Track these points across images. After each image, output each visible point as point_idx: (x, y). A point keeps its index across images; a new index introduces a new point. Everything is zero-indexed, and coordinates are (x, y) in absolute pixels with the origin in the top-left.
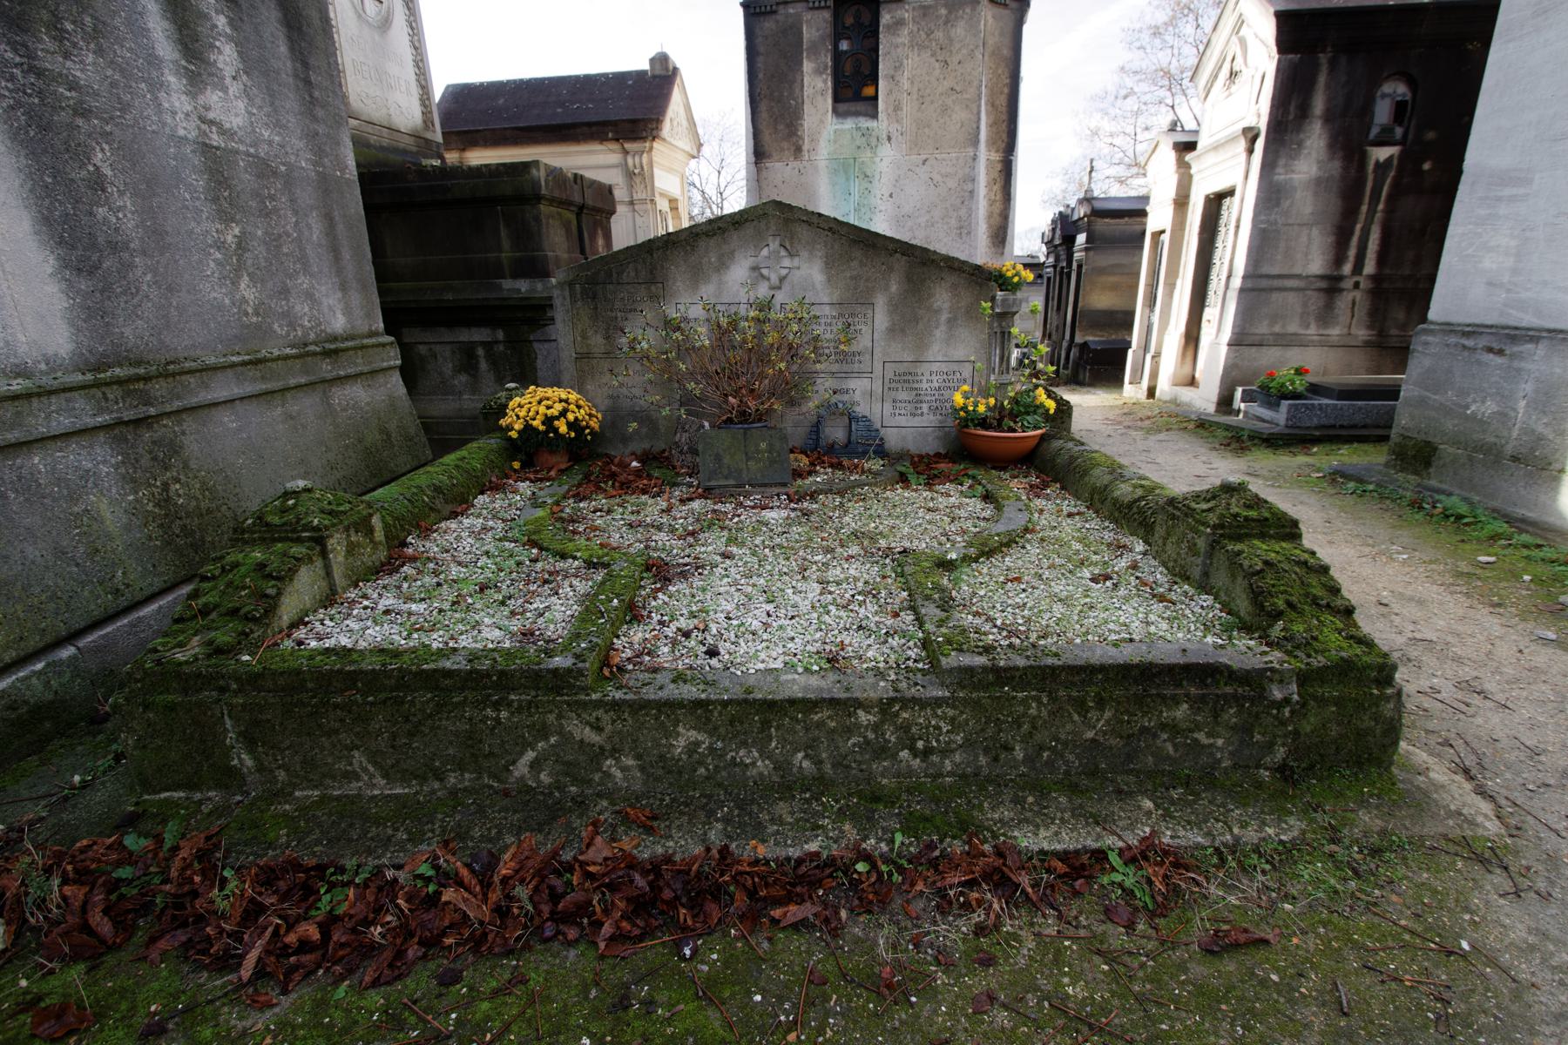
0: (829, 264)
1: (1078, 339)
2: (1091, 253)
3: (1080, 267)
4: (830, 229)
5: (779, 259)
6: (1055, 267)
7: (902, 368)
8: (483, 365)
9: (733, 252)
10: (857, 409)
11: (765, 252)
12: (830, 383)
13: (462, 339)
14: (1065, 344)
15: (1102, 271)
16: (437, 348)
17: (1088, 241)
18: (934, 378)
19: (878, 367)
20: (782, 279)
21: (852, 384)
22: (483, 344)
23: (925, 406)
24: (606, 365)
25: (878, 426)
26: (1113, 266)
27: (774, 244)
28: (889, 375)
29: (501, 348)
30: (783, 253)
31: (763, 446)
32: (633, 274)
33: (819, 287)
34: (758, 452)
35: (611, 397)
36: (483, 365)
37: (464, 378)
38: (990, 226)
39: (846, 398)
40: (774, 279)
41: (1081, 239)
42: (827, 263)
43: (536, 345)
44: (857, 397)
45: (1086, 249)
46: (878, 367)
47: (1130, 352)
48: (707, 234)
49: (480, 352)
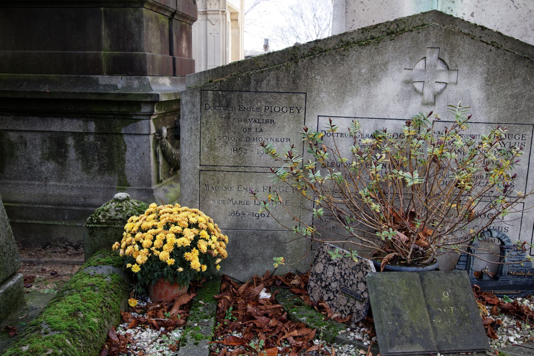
0: (489, 81)
4: (493, 44)
5: (435, 73)
8: (72, 154)
9: (386, 64)
11: (420, 65)
13: (52, 129)
16: (28, 136)
20: (436, 95)
22: (74, 134)
24: (233, 180)
27: (432, 57)
29: (92, 138)
30: (440, 66)
31: (446, 296)
32: (273, 82)
33: (476, 104)
34: (442, 304)
35: (236, 214)
36: (72, 154)
37: (51, 165)
40: (428, 94)
42: (487, 80)
43: (126, 138)
48: (359, 43)
49: (71, 141)
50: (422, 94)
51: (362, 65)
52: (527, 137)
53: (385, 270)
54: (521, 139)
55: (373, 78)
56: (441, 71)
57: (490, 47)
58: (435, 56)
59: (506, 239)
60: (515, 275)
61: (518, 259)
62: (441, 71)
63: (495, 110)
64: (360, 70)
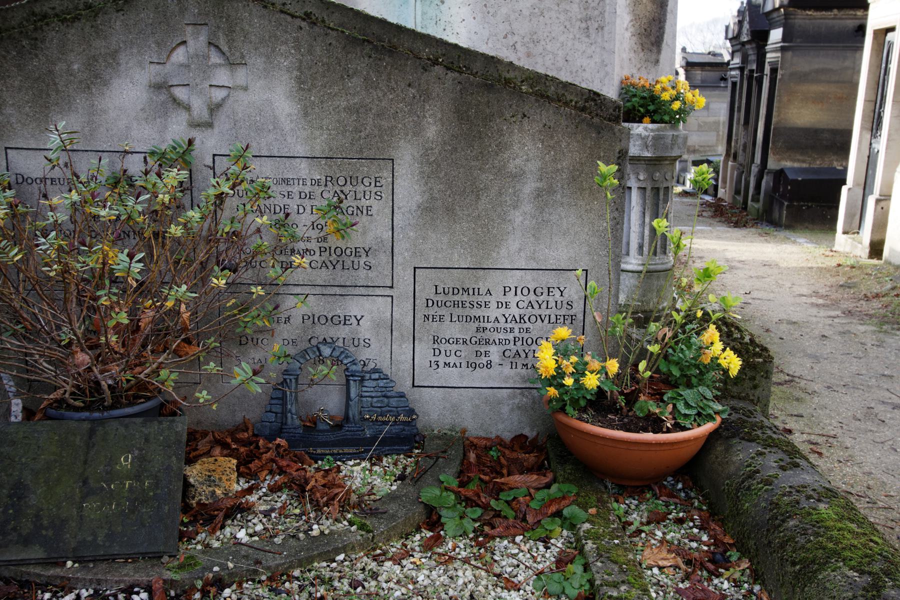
0: (304, 83)
1: (772, 164)
2: (789, 54)
3: (774, 71)
5: (206, 69)
6: (742, 69)
7: (449, 280)
9: (114, 54)
10: (364, 354)
11: (179, 56)
12: (315, 305)
14: (755, 169)
15: (803, 78)
17: (784, 39)
18: (511, 298)
19: (404, 277)
20: (214, 108)
21: (354, 307)
23: (495, 353)
25: (404, 385)
26: (817, 71)
27: (197, 42)
28: (426, 292)
30: (215, 58)
31: (126, 462)
33: (287, 125)
34: (111, 476)
38: (636, 18)
39: (342, 332)
40: (199, 106)
41: (776, 35)
42: (300, 81)
44: (365, 330)
45: (783, 49)
46: (404, 277)
47: (844, 190)
50: (188, 108)
51: (72, 57)
52: (383, 182)
53: (48, 417)
54: (373, 184)
55: (95, 77)
56: (216, 66)
57: (298, 22)
58: (203, 39)
59: (350, 360)
60: (376, 420)
61: (380, 394)
62: (216, 66)
63: (322, 135)
64: (69, 66)
